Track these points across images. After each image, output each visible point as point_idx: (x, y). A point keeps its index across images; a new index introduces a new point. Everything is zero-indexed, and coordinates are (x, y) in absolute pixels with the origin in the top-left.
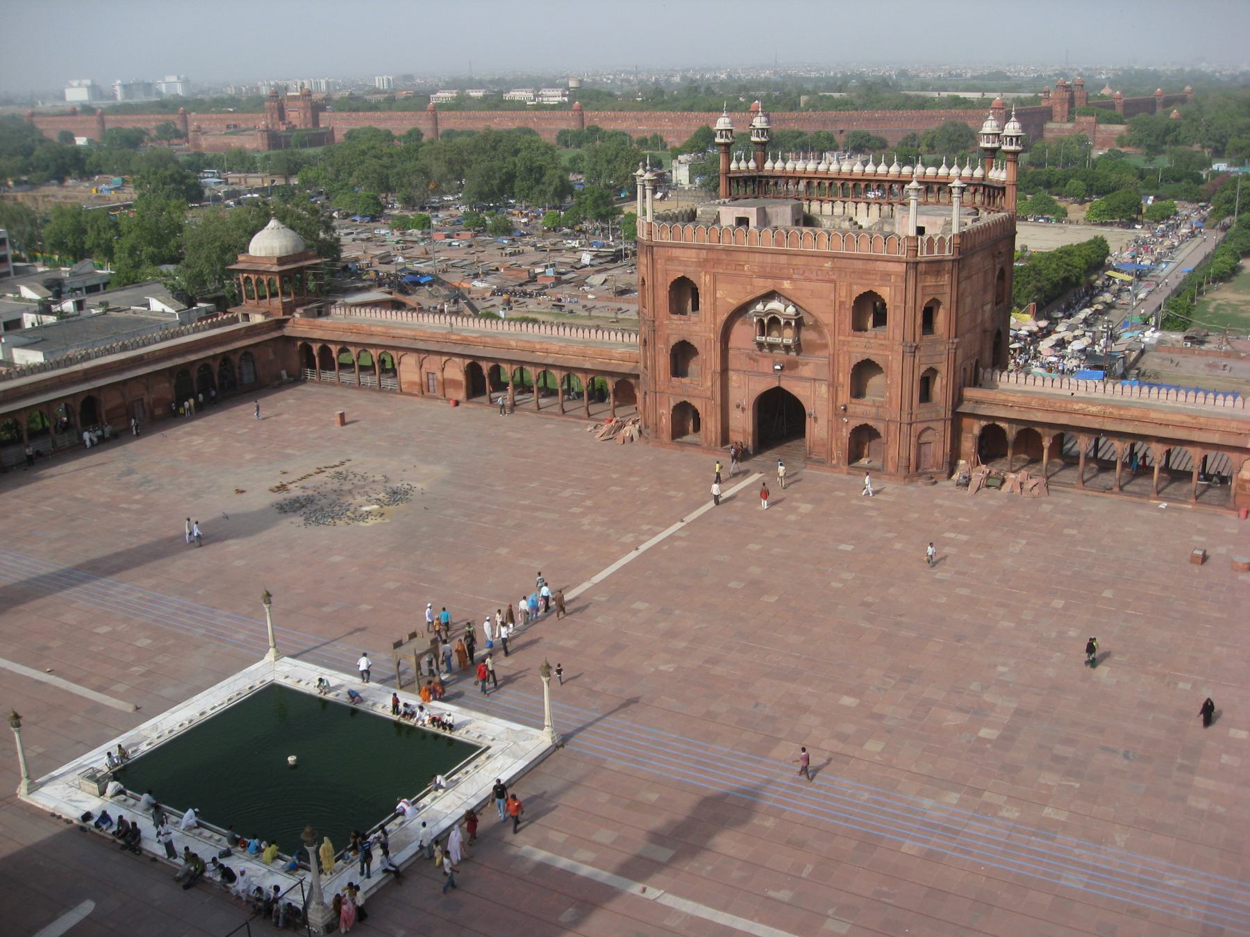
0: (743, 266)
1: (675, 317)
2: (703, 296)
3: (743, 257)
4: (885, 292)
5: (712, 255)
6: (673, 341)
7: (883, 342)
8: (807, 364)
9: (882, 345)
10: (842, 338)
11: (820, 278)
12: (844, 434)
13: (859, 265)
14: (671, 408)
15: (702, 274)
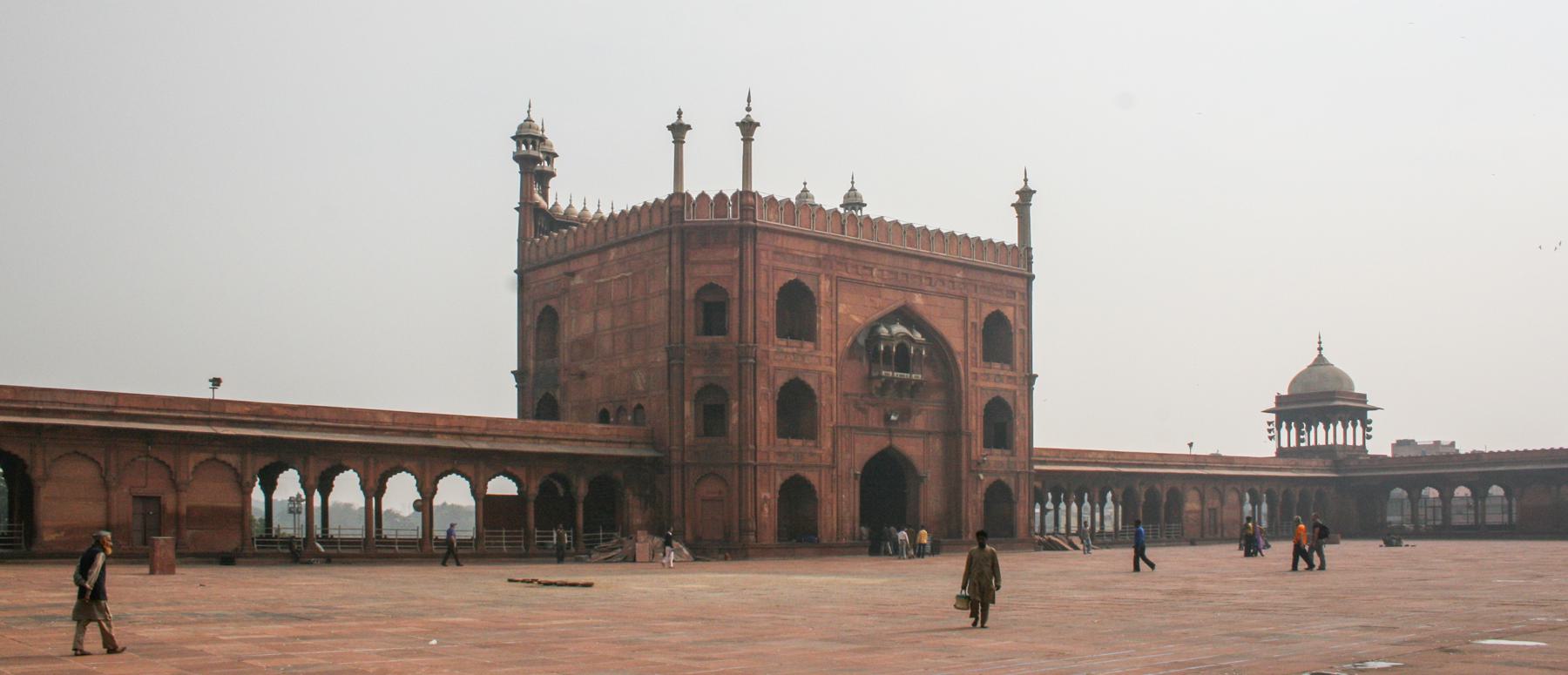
0: (871, 269)
1: (783, 342)
2: (823, 311)
3: (870, 257)
4: (1009, 312)
5: (836, 251)
6: (781, 381)
7: (1010, 373)
8: (920, 412)
9: (1010, 377)
10: (973, 370)
11: (952, 291)
12: (979, 496)
13: (988, 278)
14: (778, 488)
15: (823, 276)
